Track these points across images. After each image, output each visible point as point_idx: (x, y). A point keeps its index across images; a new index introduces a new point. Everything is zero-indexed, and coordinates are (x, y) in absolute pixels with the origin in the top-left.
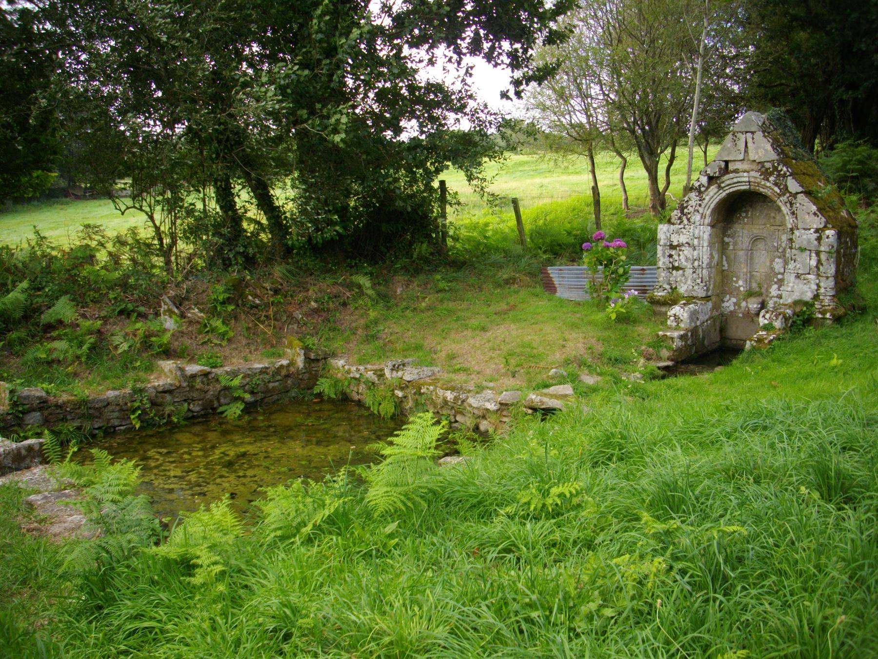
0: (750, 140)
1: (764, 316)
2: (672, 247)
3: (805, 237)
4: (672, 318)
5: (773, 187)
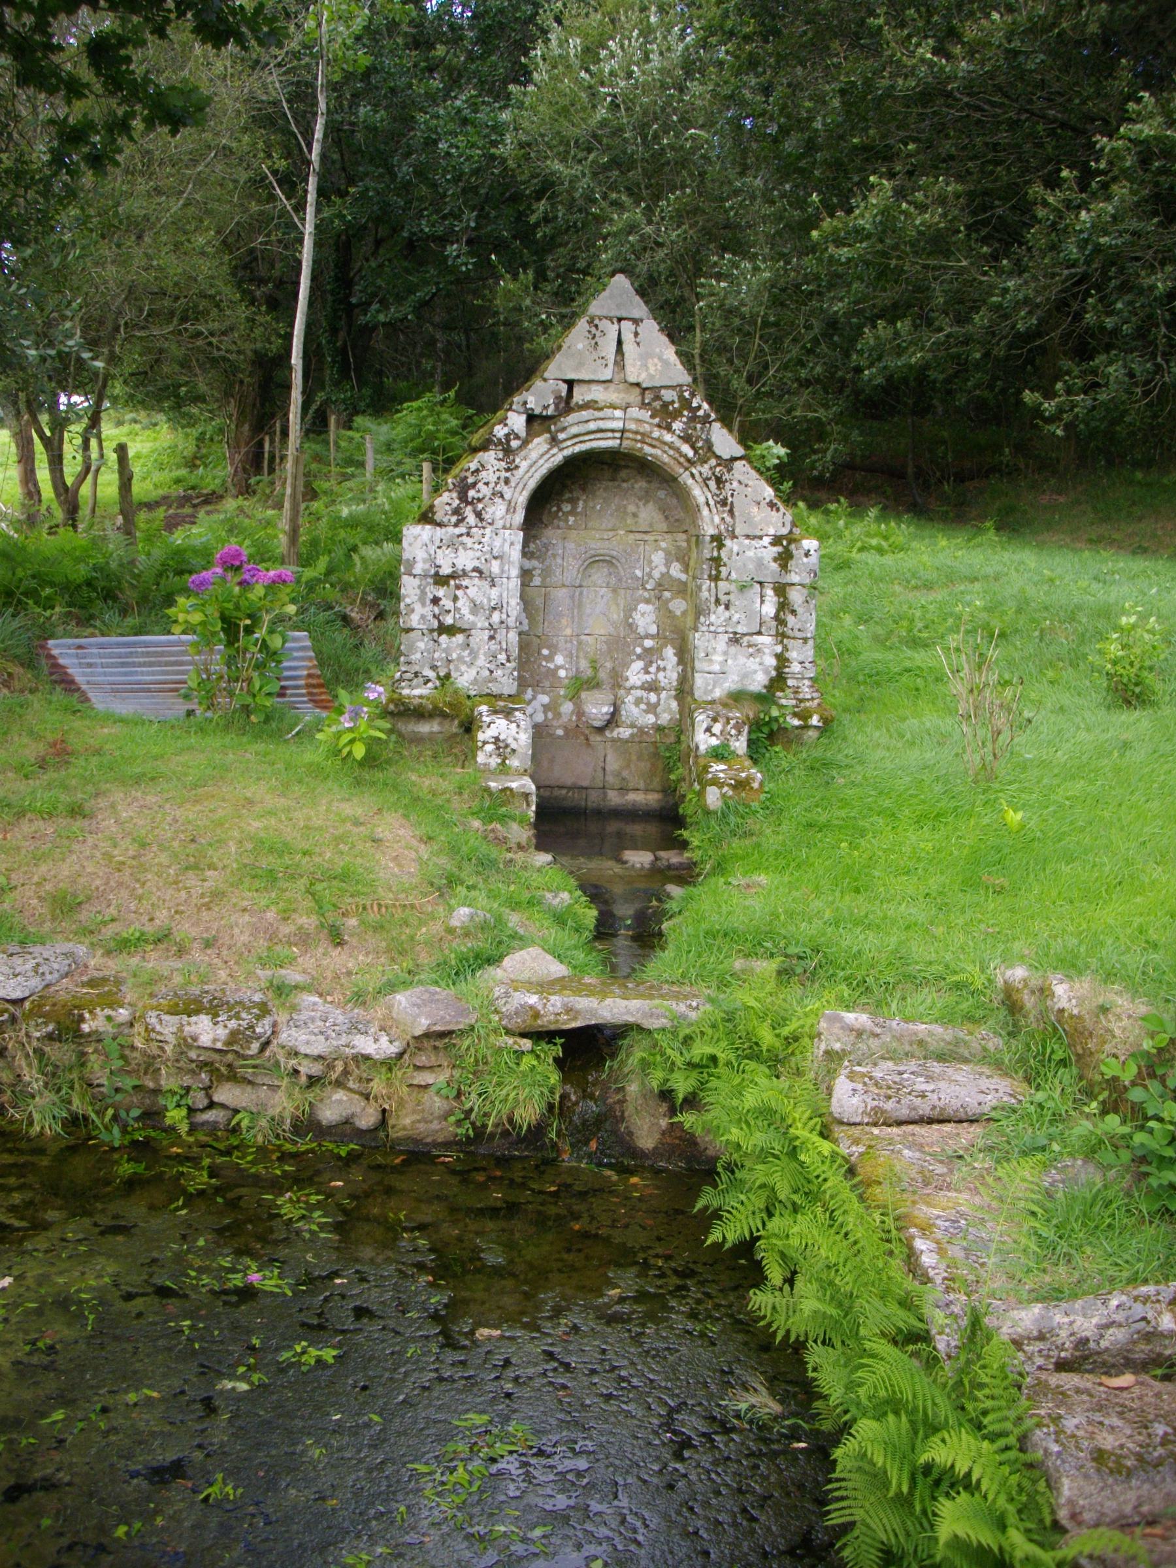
0: (628, 337)
1: (708, 730)
2: (441, 580)
3: (750, 553)
4: (489, 748)
5: (678, 443)
